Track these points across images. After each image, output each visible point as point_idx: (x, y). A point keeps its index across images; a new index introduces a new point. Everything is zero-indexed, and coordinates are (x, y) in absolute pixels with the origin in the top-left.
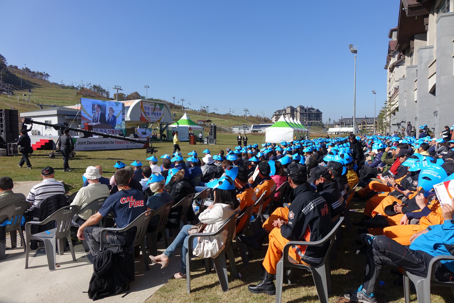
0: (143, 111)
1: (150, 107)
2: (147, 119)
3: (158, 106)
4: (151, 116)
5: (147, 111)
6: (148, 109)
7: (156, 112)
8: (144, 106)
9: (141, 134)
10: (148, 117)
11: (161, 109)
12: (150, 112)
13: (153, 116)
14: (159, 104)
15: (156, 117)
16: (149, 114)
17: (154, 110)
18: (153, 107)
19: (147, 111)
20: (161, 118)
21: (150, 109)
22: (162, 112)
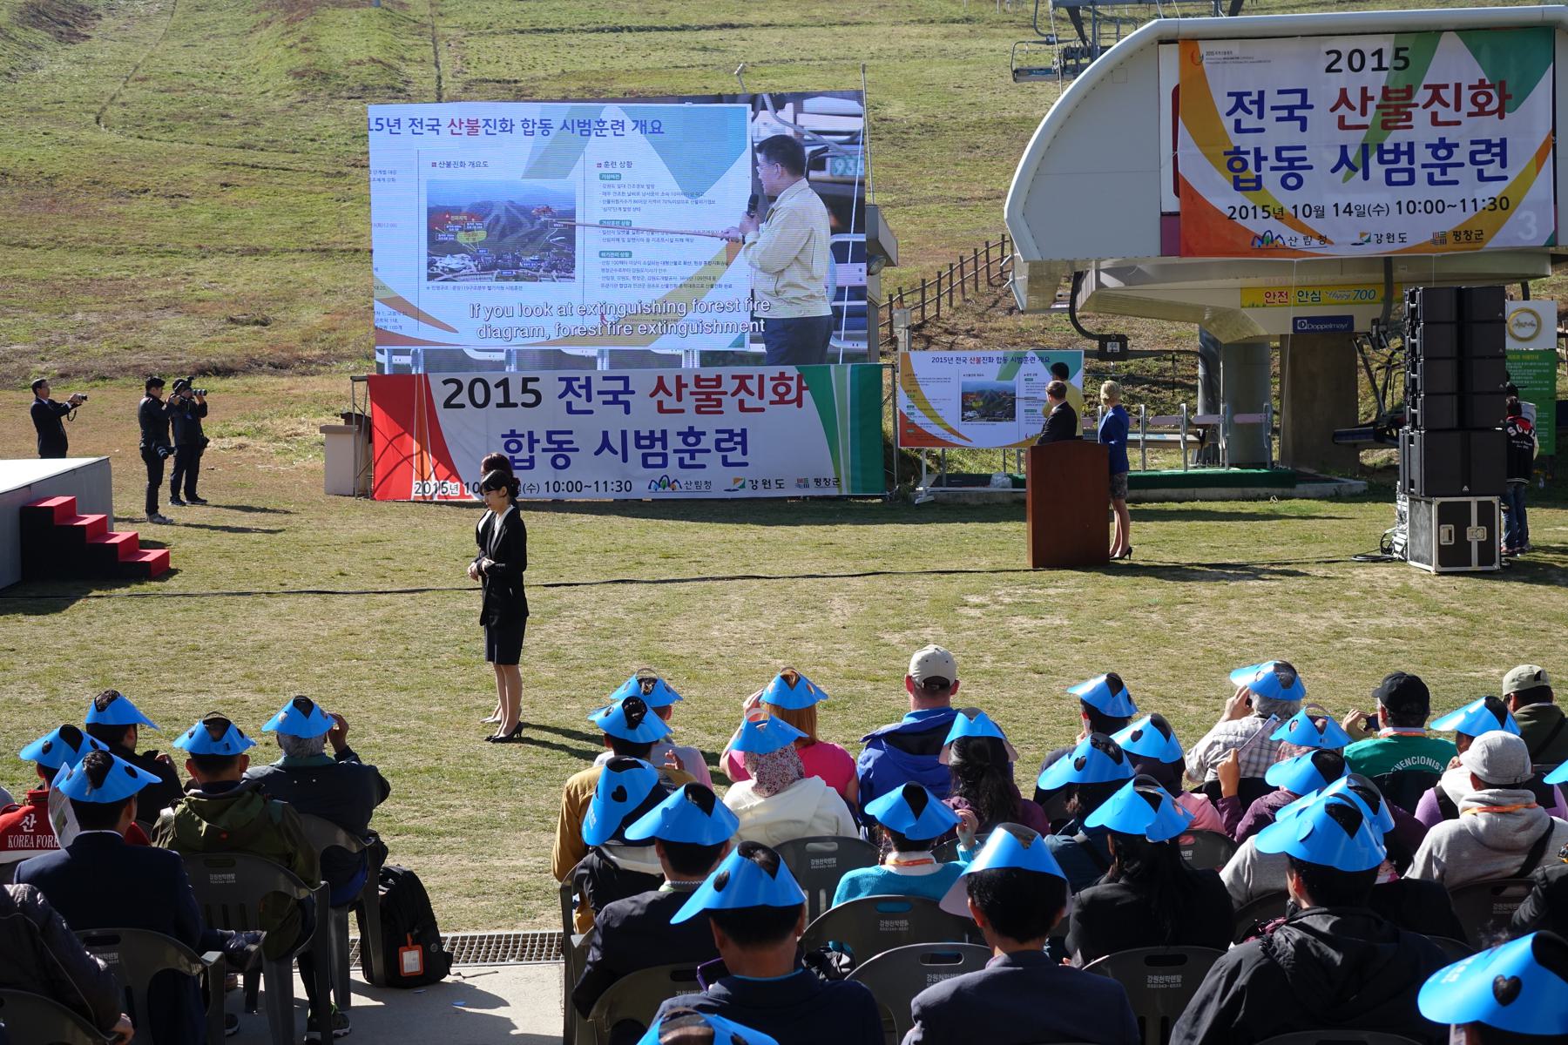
0: (1207, 138)
1: (1325, 90)
2: (1257, 225)
3: (1455, 65)
4: (1324, 187)
5: (1278, 133)
6: (1296, 111)
7: (1421, 131)
8: (1221, 82)
9: (951, 410)
10: (1286, 200)
11: (1501, 95)
12: (1322, 141)
13: (1373, 191)
14: (1471, 33)
15: (1421, 191)
16: (1293, 168)
17: (1396, 107)
18: (1375, 82)
19: (1278, 133)
20: (1502, 205)
21: (1321, 117)
22: (1528, 124)
